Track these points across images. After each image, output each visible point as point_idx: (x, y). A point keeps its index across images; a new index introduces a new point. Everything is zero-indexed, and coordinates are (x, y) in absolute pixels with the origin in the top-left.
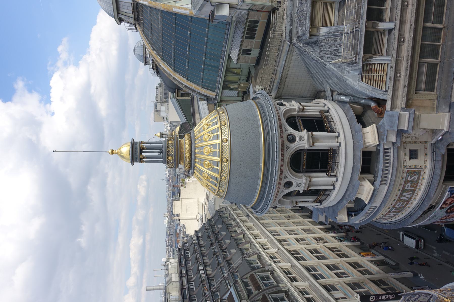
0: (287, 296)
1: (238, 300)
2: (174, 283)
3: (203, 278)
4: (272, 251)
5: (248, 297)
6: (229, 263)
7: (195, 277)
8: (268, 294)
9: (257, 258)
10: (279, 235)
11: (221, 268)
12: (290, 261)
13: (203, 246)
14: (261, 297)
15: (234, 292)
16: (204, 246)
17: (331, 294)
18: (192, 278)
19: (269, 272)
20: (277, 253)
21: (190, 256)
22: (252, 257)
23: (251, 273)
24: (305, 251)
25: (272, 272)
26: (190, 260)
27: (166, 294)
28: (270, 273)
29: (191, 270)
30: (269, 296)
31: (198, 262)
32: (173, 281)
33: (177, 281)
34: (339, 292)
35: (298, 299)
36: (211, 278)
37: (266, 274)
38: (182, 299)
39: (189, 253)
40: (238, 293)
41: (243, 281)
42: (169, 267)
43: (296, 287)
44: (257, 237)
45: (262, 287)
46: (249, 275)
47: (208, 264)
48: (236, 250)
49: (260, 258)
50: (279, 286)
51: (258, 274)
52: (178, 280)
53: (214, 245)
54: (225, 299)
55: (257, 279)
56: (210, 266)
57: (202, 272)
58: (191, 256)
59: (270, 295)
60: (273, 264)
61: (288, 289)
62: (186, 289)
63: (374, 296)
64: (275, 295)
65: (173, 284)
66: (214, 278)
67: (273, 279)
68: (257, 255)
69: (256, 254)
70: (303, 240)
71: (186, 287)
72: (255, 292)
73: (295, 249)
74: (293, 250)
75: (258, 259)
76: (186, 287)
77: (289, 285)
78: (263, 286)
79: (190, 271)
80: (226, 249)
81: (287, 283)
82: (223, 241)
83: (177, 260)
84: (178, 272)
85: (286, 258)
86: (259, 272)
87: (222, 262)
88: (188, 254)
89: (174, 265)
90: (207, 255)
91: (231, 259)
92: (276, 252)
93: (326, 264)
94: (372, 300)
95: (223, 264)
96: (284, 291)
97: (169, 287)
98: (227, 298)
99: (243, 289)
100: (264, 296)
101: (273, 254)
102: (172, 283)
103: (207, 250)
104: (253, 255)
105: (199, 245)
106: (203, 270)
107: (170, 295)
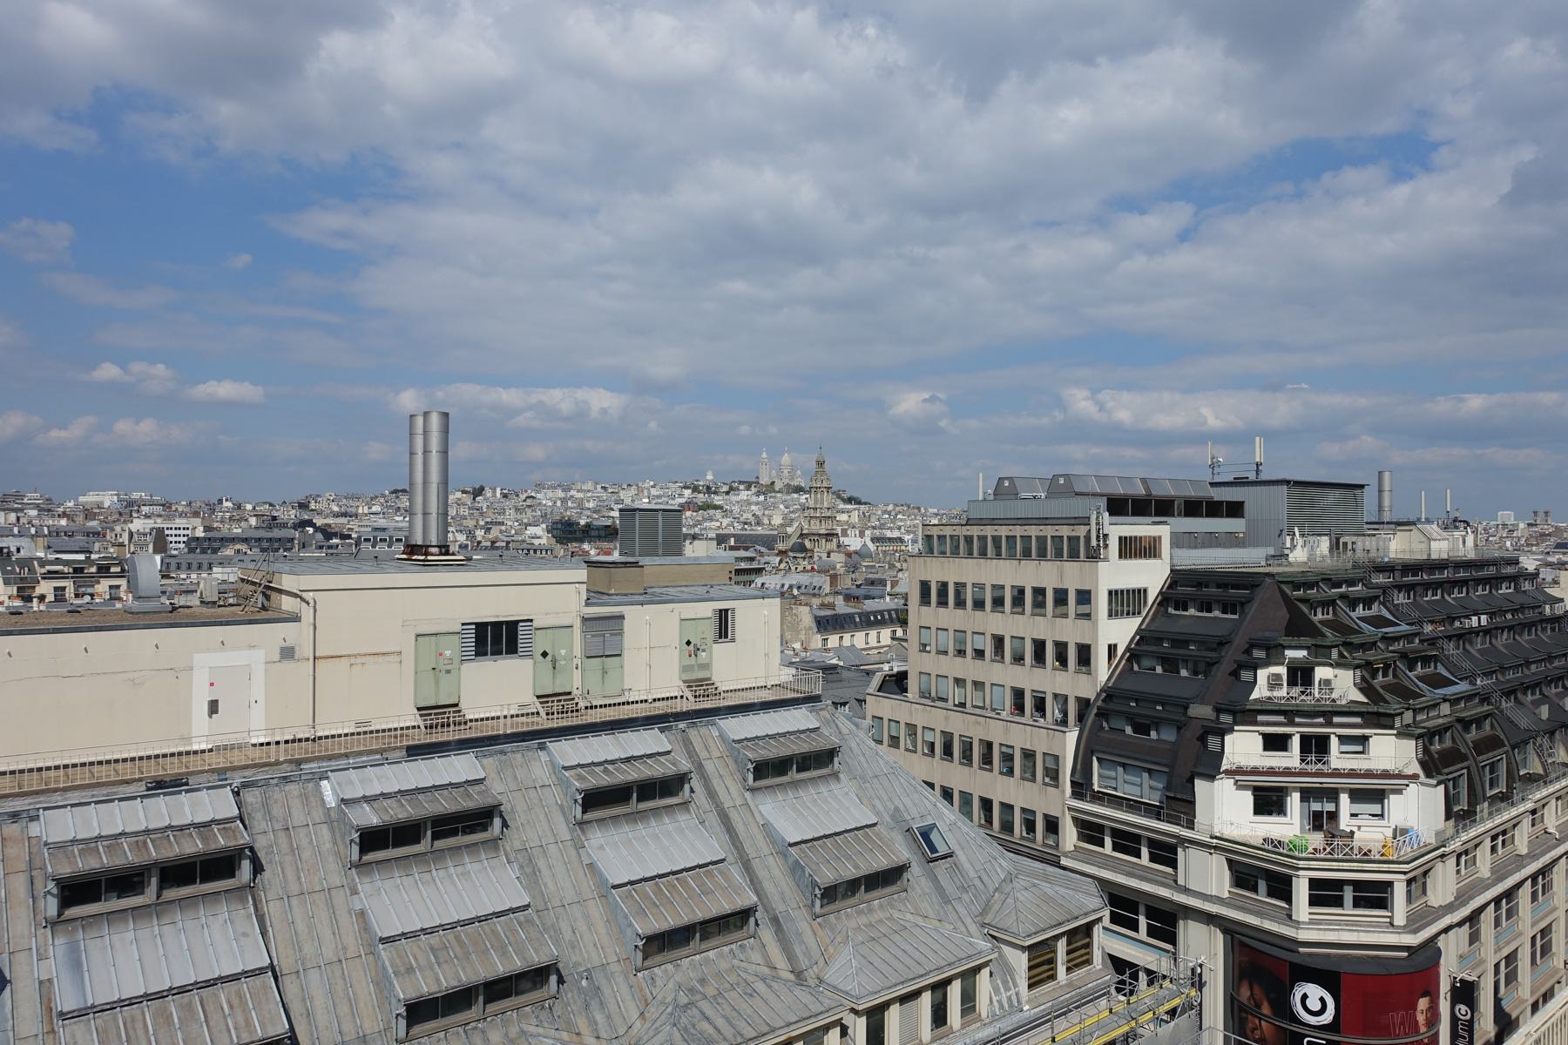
0: (1461, 813)
1: (1451, 695)
2: (1424, 546)
3: (1457, 624)
4: (1522, 841)
5: (1459, 720)
6: (1508, 694)
7: (1452, 602)
8: (1468, 768)
9: (1531, 772)
10: (1497, 923)
11: (1542, 660)
12: (1532, 856)
13: (1538, 632)
14: (1463, 750)
15: (1457, 691)
16: (1536, 634)
17: (1465, 923)
18: (1450, 595)
19: (1507, 789)
20: (1546, 832)
21: (1500, 592)
22: (1536, 759)
23: (1506, 743)
24: (1546, 916)
25: (1506, 798)
26: (1490, 591)
27: (1393, 526)
28: (1504, 791)
29: (1468, 593)
30: (1462, 769)
31: (1494, 613)
32: (1432, 543)
33: (1429, 555)
34: (1466, 948)
35: (1474, 829)
36: (1461, 642)
37: (1503, 781)
38: (1402, 566)
39: (1509, 591)
40: (1461, 698)
41: (1486, 717)
42: (1455, 533)
43: (1518, 823)
44: (1463, 858)
45: (1481, 758)
46: (1502, 737)
47: (1494, 641)
48: (1548, 719)
49: (1532, 779)
50: (1484, 801)
51: (1505, 760)
52: (1433, 557)
53: (1547, 664)
54: (1436, 668)
55: (1490, 754)
56: (1511, 641)
57: (1474, 621)
58: (1501, 594)
59: (1465, 771)
60: (1529, 805)
61: (1478, 820)
62: (1419, 578)
63: (1468, 1017)
64: (1464, 782)
65: (1421, 542)
66: (1461, 650)
67: (1492, 794)
68: (1542, 772)
69: (1545, 770)
70: (1546, 950)
71: (1425, 577)
72: (1473, 734)
73: (1555, 889)
74: (1552, 879)
75: (1528, 773)
76: (1425, 577)
77: (1489, 825)
78: (1484, 759)
79: (1464, 589)
80: (1544, 695)
81: (1493, 822)
82: (1560, 689)
83: (1471, 555)
84: (1451, 559)
85: (1536, 849)
86: (1507, 764)
87: (1507, 678)
88: (1507, 588)
89: (1461, 546)
90: (1514, 639)
91: (1521, 704)
92: (1550, 830)
93: (1519, 956)
94: (1460, 1009)
95: (1502, 680)
96: (1471, 809)
97: (1415, 532)
98: (1439, 674)
99: (1472, 713)
100: (1464, 758)
101: (1543, 821)
102: (1427, 541)
103: (1527, 641)
104: (1542, 763)
105: (1542, 621)
106: (1480, 626)
107: (1392, 536)
